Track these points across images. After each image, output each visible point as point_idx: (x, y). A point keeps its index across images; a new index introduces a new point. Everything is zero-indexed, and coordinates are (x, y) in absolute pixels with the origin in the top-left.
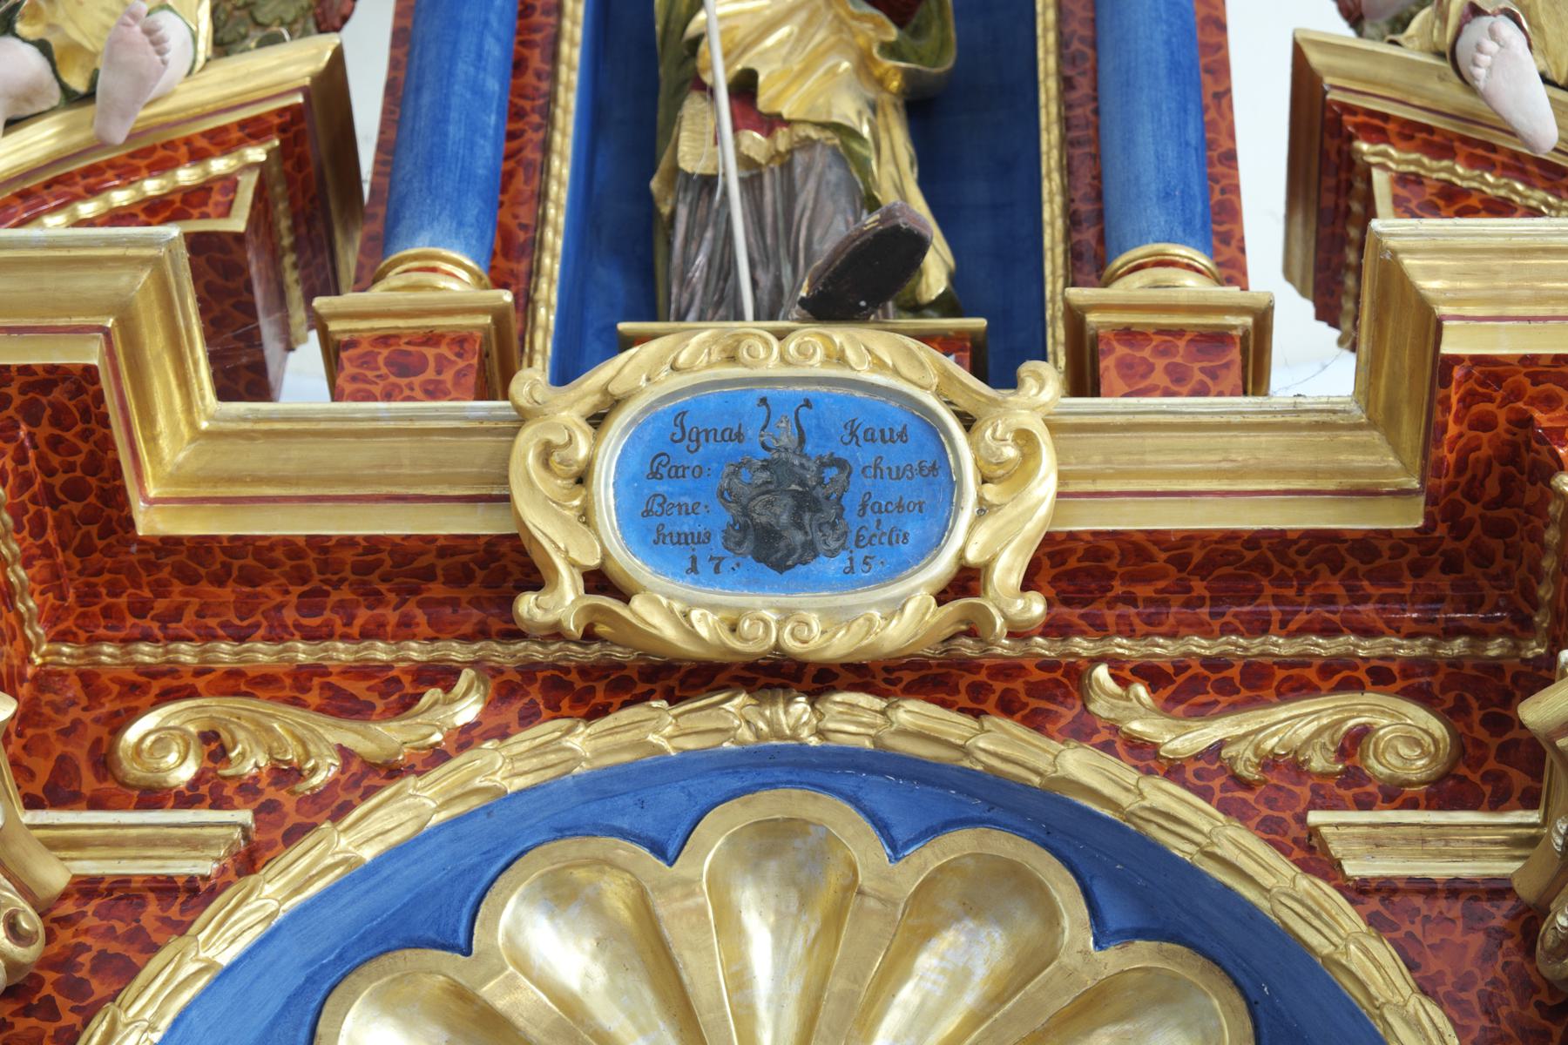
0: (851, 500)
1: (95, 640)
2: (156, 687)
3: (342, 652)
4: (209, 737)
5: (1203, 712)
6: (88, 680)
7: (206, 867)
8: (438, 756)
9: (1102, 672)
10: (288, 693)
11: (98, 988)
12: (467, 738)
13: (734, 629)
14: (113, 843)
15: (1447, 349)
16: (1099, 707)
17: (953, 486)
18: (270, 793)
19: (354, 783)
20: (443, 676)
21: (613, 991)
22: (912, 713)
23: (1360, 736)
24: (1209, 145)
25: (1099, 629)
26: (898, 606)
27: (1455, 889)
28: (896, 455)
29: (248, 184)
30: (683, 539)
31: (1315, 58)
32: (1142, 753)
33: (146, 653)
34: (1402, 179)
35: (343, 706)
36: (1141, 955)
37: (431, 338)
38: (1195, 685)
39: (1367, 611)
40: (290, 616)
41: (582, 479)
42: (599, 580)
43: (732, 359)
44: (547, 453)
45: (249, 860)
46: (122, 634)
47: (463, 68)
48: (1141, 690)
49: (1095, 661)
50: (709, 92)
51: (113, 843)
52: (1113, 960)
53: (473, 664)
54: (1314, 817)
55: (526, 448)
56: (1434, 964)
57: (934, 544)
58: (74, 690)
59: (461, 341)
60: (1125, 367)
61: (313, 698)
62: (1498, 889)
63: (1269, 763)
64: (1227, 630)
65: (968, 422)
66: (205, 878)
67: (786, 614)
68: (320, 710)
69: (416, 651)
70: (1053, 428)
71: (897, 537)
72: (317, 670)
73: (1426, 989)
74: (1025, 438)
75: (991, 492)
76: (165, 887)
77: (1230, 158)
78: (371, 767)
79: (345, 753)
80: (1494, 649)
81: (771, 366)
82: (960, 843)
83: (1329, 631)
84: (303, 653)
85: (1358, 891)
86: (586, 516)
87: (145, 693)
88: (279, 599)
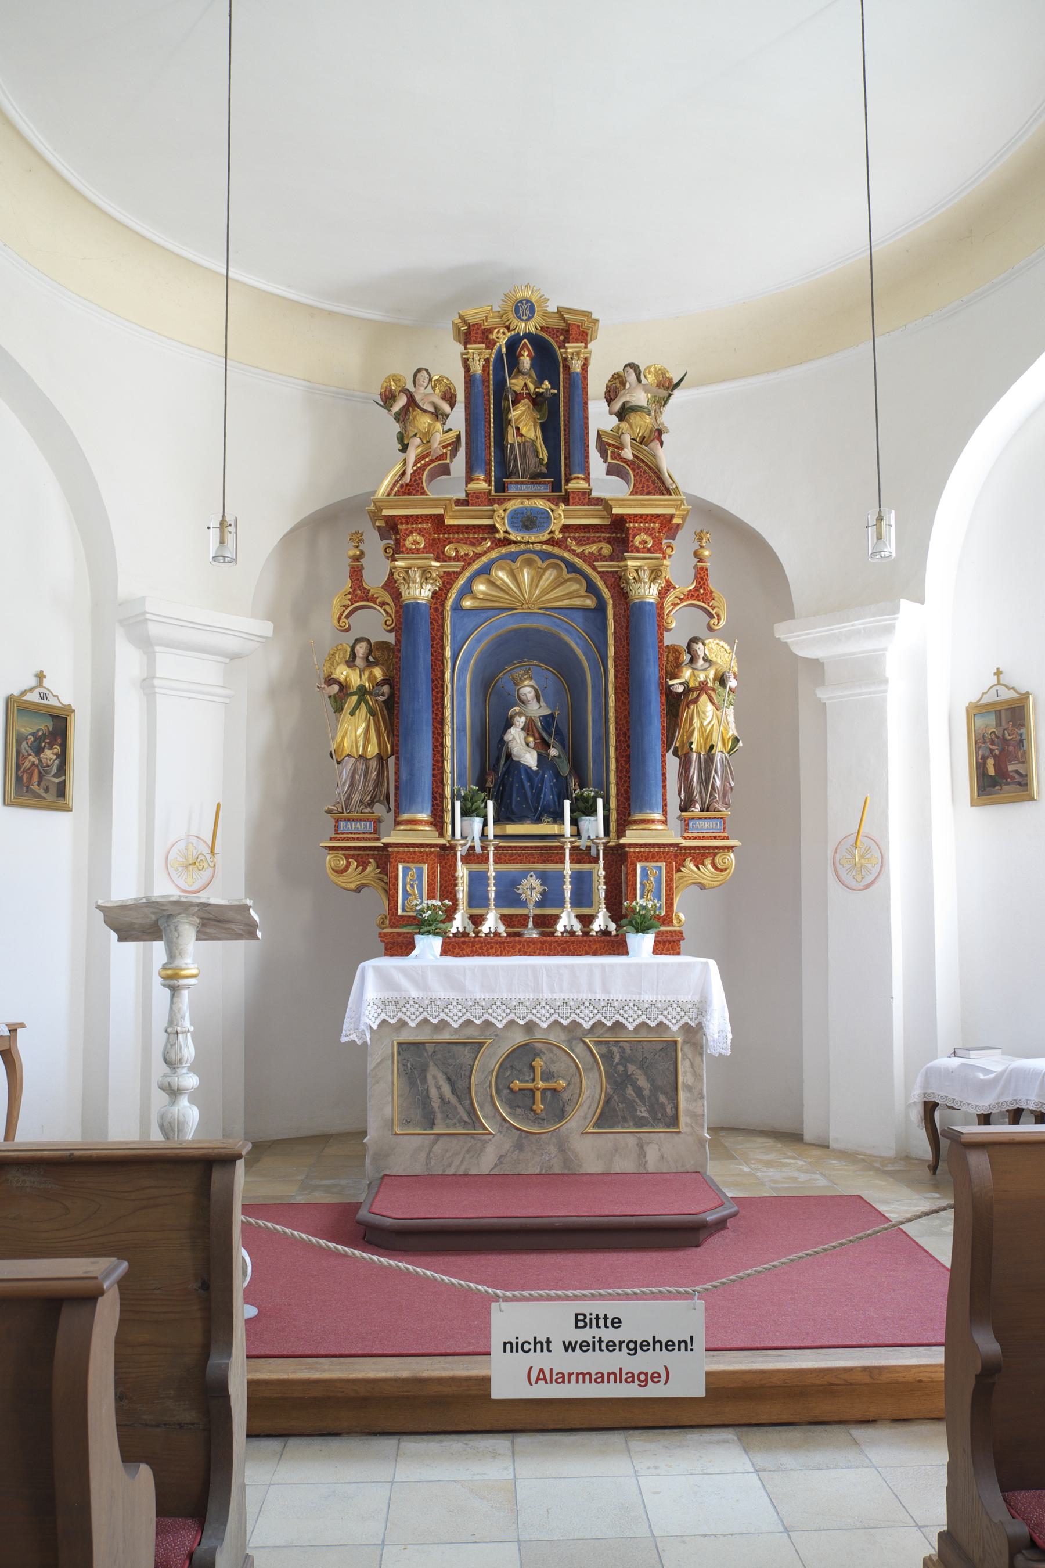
0: (537, 522)
1: (439, 534)
2: (448, 541)
3: (471, 536)
4: (456, 549)
5: (581, 545)
6: (439, 539)
7: (458, 570)
8: (485, 553)
9: (569, 539)
11: (448, 587)
12: (489, 549)
13: (523, 538)
14: (447, 567)
15: (613, 512)
16: (568, 543)
17: (551, 519)
19: (475, 556)
20: (484, 539)
21: (508, 577)
22: (544, 547)
23: (602, 548)
24: (585, 443)
25: (570, 533)
26: (543, 536)
27: (611, 572)
28: (543, 516)
29: (449, 452)
30: (516, 527)
31: (600, 433)
32: (573, 552)
33: (446, 536)
34: (612, 452)
35: (473, 544)
36: (573, 575)
37: (480, 493)
38: (581, 540)
39: (603, 530)
41: (503, 519)
42: (506, 532)
43: (522, 503)
44: (498, 516)
45: (464, 569)
47: (479, 439)
48: (574, 543)
49: (569, 537)
50: (512, 427)
51: (447, 567)
52: (570, 576)
53: (489, 538)
54: (595, 563)
55: (496, 514)
56: (608, 583)
57: (548, 527)
58: (437, 541)
59: (484, 493)
60: (573, 497)
61: (468, 542)
62: (616, 572)
63: (589, 553)
64: (585, 532)
65: (552, 511)
67: (529, 537)
68: (469, 545)
69: (481, 536)
70: (563, 511)
71: (543, 526)
72: (468, 538)
73: (607, 587)
74: (560, 515)
75: (555, 521)
76: (454, 572)
77: (588, 446)
78: (477, 554)
79: (473, 551)
80: (619, 535)
81: (528, 506)
82: (551, 561)
83: (598, 532)
84: (466, 536)
85: (599, 573)
86: (504, 524)
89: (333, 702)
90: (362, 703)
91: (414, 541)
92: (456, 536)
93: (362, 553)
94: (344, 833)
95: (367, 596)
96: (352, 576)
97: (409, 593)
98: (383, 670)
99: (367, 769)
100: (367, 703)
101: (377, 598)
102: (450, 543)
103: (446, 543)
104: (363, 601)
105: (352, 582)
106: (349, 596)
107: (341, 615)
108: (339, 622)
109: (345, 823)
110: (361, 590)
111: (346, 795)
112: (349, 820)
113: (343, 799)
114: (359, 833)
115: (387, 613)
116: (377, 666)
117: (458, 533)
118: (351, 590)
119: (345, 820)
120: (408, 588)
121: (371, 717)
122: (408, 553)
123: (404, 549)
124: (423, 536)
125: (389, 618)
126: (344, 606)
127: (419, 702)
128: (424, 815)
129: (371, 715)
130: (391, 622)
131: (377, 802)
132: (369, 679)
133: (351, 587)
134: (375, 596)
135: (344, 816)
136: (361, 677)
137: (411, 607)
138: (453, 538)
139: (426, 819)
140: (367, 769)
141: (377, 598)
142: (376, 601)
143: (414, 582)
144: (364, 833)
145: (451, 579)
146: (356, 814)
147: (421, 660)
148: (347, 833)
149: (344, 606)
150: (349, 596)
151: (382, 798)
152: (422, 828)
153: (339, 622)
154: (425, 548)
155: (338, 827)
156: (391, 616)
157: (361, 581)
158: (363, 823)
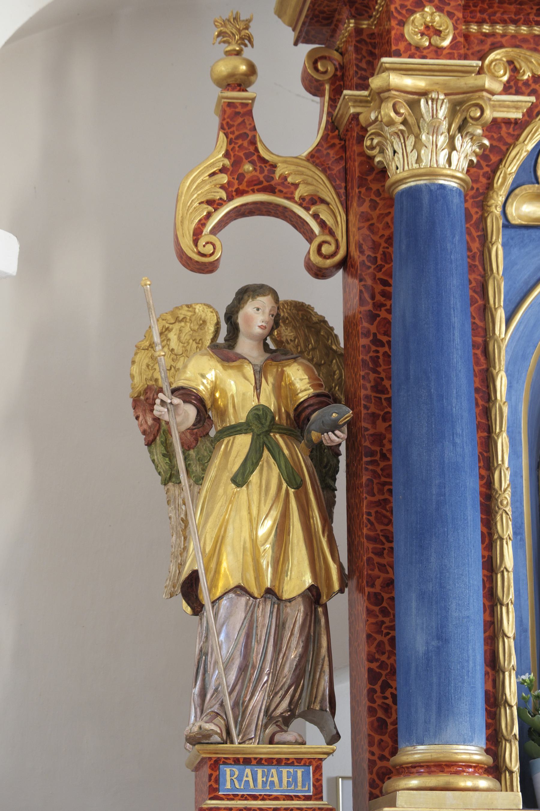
4: (510, 62)
7: (519, 115)
10: (532, 46)
18: (533, 86)
40: (532, 17)
46: (475, 20)
66: (519, 119)
76: (507, 122)
87: (486, 44)
88: (529, 11)
89: (159, 457)
90: (266, 453)
91: (427, 27)
92: (512, 29)
93: (252, 70)
94: (234, 797)
95: (270, 178)
96: (230, 126)
97: (419, 160)
98: (308, 370)
99: (280, 627)
100: (276, 453)
101: (296, 186)
102: (495, 47)
103: (487, 47)
104: (260, 191)
105: (230, 142)
106: (224, 179)
107: (202, 224)
108: (196, 242)
109: (236, 770)
110: (252, 163)
111: (235, 694)
112: (247, 762)
113: (229, 704)
114: (276, 798)
115: (322, 224)
116: (295, 359)
117: (515, 22)
118: (227, 162)
119: (237, 761)
120: (418, 145)
121: (291, 491)
122: (411, 57)
123: (402, 46)
124: (450, 15)
125: (328, 238)
126: (210, 202)
127: (454, 444)
128: (472, 749)
129: (289, 484)
130: (332, 248)
132: (278, 389)
133: (227, 155)
134: (290, 180)
136: (258, 388)
137: (426, 199)
138: (503, 35)
139: (477, 758)
140: (280, 627)
141: (296, 186)
142: (293, 193)
143: (435, 130)
144: (290, 798)
145: (501, 139)
147: (457, 334)
148: (244, 798)
149: (210, 202)
150: (224, 179)
152: (469, 783)
153: (196, 242)
154: (454, 45)
155: (217, 781)
156: (331, 233)
157: (253, 142)
158: (285, 771)
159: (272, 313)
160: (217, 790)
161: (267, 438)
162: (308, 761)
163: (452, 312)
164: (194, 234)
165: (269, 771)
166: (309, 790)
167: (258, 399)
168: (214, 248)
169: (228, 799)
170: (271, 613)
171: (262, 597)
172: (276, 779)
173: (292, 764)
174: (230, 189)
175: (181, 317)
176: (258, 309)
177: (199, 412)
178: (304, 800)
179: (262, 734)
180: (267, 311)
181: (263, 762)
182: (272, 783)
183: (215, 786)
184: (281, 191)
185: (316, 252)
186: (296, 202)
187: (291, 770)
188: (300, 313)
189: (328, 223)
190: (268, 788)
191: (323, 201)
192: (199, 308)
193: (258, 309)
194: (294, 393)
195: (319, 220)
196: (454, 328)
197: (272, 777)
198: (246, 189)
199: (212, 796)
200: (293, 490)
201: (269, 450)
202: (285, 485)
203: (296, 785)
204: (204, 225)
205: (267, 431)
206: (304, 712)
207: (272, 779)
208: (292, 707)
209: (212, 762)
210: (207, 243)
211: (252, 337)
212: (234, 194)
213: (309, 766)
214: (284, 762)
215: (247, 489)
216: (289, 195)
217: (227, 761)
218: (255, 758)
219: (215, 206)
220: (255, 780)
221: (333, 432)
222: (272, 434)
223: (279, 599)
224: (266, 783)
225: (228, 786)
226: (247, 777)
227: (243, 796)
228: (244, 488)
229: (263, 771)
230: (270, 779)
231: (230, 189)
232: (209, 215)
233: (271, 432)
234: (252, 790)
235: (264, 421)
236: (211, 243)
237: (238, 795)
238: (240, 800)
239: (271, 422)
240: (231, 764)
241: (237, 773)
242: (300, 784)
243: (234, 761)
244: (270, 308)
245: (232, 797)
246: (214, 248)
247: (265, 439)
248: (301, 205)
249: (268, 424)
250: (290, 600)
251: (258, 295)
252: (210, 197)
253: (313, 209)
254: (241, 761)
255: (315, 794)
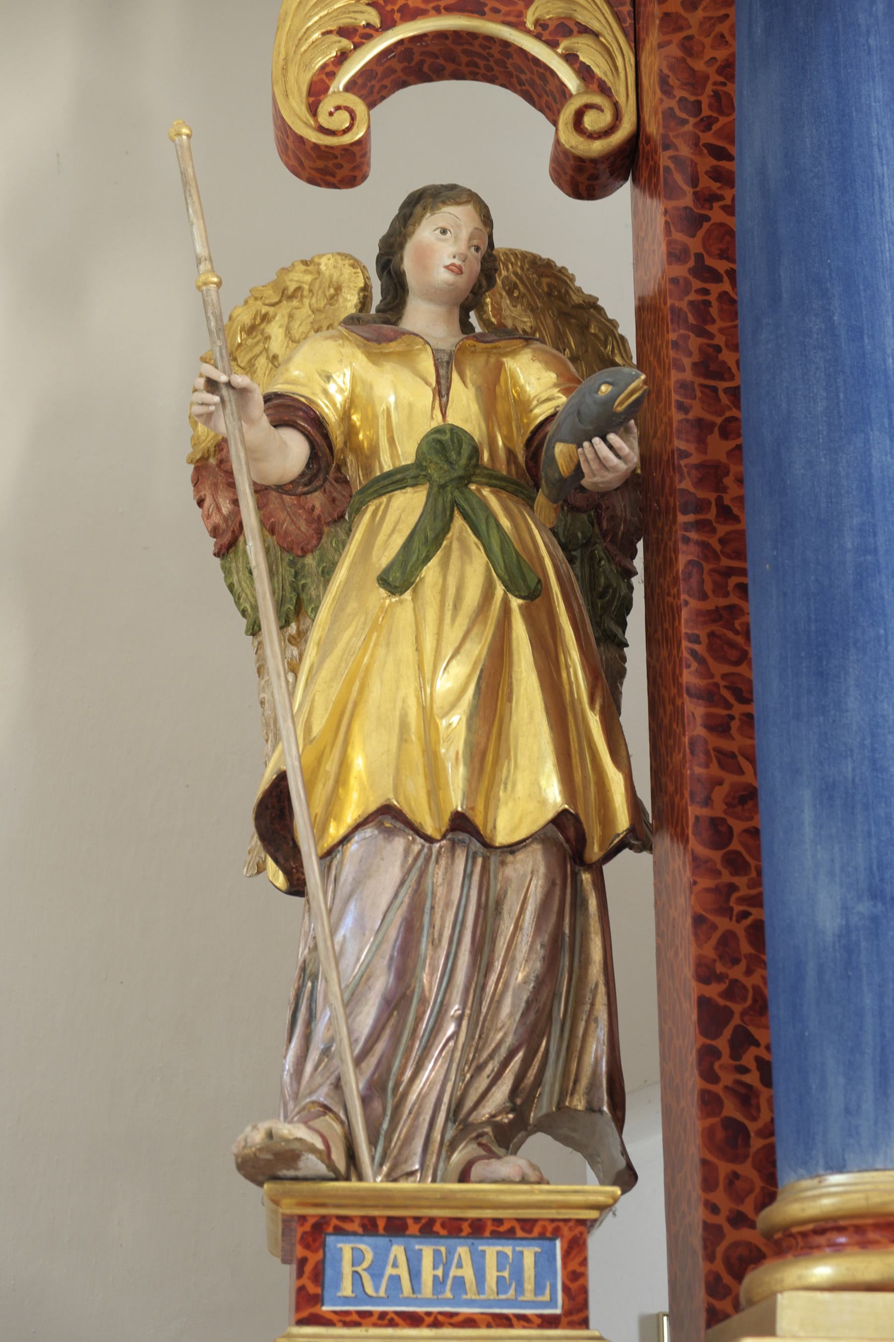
90: (459, 522)
107: (329, 72)
108: (313, 109)
109: (367, 1247)
111: (372, 1061)
113: (354, 1086)
115: (585, 73)
119: (369, 1227)
121: (516, 603)
125: (598, 99)
126: (343, 32)
129: (511, 587)
130: (606, 118)
131: (541, 1127)
135: (362, 1199)
136: (442, 391)
142: (521, 15)
146: (428, 1185)
149: (343, 32)
151: (579, 1103)
155: (318, 1276)
158: (491, 1251)
159: (475, 242)
160: (318, 1299)
161: (462, 492)
162: (550, 1227)
163: (876, 154)
164: (310, 93)
165: (450, 1252)
166: (552, 1303)
167: (444, 415)
168: (353, 118)
169: (346, 1324)
170: (467, 876)
171: (444, 837)
172: (468, 1273)
173: (509, 1235)
174: (389, 8)
175: (292, 287)
176: (444, 231)
177: (314, 456)
178: (541, 1326)
179: (441, 1165)
180: (464, 234)
181: (437, 1227)
182: (460, 1282)
183: (312, 1289)
184: (496, 11)
185: (570, 126)
186: (528, 32)
187: (508, 1250)
188: (545, 281)
189: (596, 70)
190: (448, 1294)
191: (585, 30)
192: (326, 264)
193: (444, 231)
194: (523, 405)
195: (577, 66)
196: (881, 187)
197: (460, 1266)
198: (423, 6)
199: (305, 1314)
200: (520, 601)
201: (466, 517)
202: (500, 590)
203: (520, 1289)
204: (332, 75)
205: (461, 478)
206: (548, 1115)
207: (459, 1273)
208: (519, 1101)
209: (307, 1227)
210: (338, 108)
211: (433, 295)
212: (397, 16)
213: (553, 1239)
214: (489, 1228)
215: (414, 599)
216: (511, 19)
217: (348, 1227)
218: (417, 1219)
219: (357, 39)
220: (415, 1274)
221: (604, 439)
222: (473, 487)
223: (488, 845)
224: (444, 1282)
225: (347, 1289)
226: (395, 1265)
227: (383, 1315)
228: (407, 595)
229: (437, 1253)
230: (454, 1272)
231: (389, 8)
232: (342, 57)
233: (470, 482)
234: (407, 1301)
235: (453, 455)
236: (347, 109)
237: (370, 1314)
238: (375, 1325)
239: (470, 458)
240: (354, 1234)
241: (369, 1256)
242: (529, 1285)
243: (364, 1226)
244: (471, 229)
245: (355, 1317)
246: (353, 118)
247: (457, 494)
248: (538, 37)
249: (463, 461)
250: (512, 848)
251: (444, 203)
252: (345, 21)
253: (564, 44)
254: (381, 1224)
255: (568, 1312)
